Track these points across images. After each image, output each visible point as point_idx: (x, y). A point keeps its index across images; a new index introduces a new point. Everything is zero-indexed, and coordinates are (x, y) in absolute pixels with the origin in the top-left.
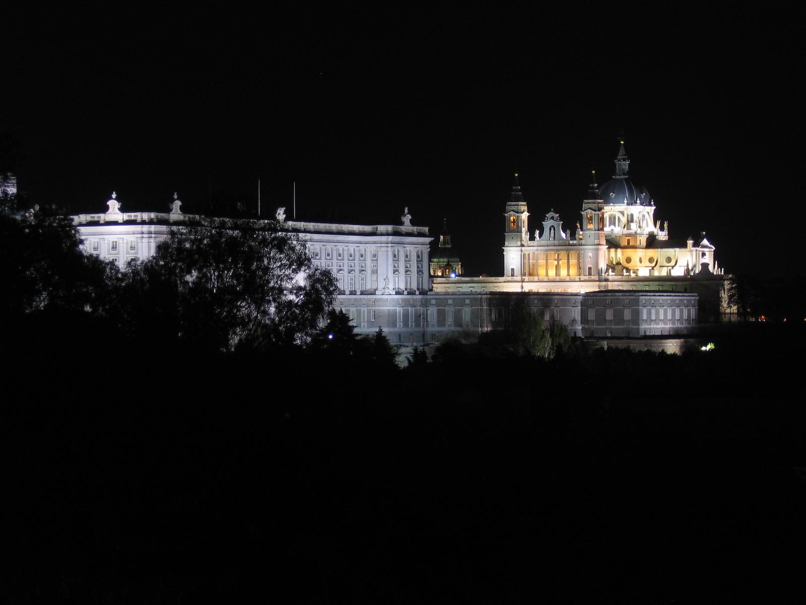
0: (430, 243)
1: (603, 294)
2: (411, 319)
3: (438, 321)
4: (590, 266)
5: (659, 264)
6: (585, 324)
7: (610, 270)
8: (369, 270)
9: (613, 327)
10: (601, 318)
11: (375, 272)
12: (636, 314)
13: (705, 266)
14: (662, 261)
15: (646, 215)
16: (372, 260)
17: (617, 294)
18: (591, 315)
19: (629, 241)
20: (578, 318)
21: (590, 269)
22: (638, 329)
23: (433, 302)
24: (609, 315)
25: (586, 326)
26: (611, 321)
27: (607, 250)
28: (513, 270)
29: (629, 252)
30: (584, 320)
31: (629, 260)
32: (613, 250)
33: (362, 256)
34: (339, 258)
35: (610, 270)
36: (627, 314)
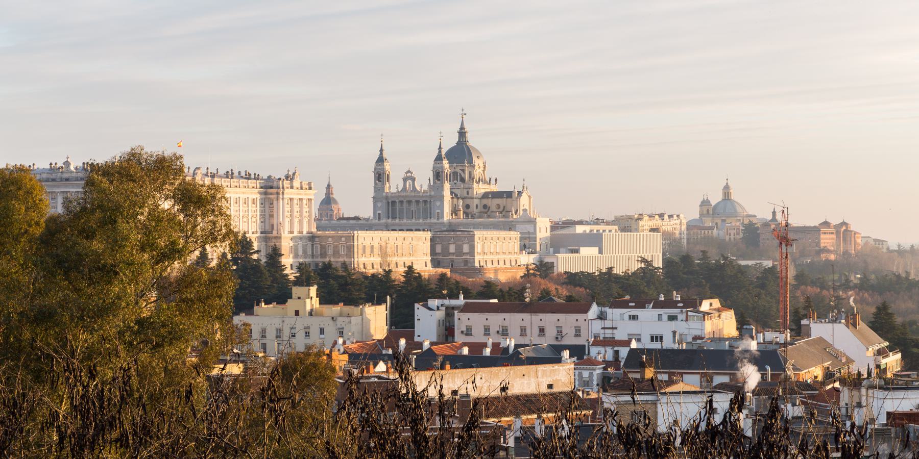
0: (314, 195)
1: (447, 233)
2: (300, 252)
3: (321, 254)
4: (437, 211)
5: (490, 211)
6: (433, 256)
7: (454, 215)
8: (267, 216)
9: (454, 257)
10: (446, 251)
11: (271, 216)
12: (472, 248)
13: (525, 210)
14: (493, 208)
15: (482, 172)
16: (270, 207)
17: (458, 233)
18: (439, 249)
19: (468, 192)
20: (429, 251)
21: (438, 213)
22: (474, 259)
23: (317, 239)
24: (452, 249)
25: (435, 257)
26: (453, 254)
27: (450, 199)
28: (379, 214)
29: (468, 201)
30: (433, 252)
31: (468, 207)
32: (455, 200)
33: (262, 204)
34: (245, 205)
35: (454, 215)
36: (466, 249)
